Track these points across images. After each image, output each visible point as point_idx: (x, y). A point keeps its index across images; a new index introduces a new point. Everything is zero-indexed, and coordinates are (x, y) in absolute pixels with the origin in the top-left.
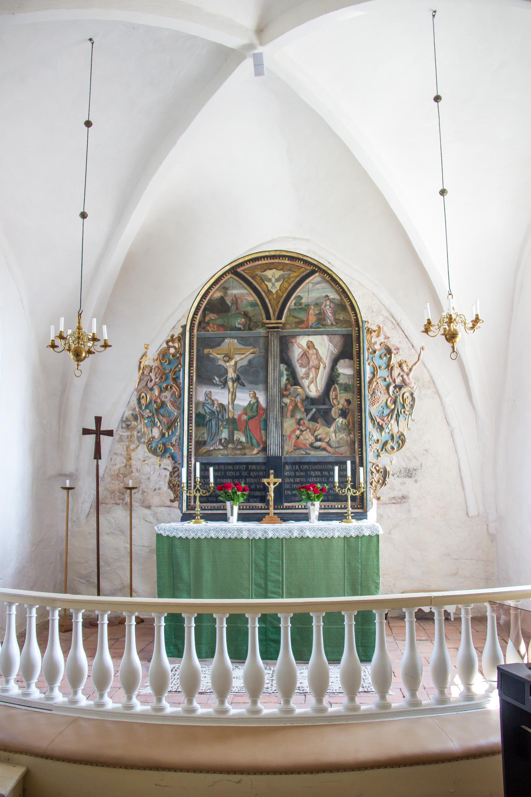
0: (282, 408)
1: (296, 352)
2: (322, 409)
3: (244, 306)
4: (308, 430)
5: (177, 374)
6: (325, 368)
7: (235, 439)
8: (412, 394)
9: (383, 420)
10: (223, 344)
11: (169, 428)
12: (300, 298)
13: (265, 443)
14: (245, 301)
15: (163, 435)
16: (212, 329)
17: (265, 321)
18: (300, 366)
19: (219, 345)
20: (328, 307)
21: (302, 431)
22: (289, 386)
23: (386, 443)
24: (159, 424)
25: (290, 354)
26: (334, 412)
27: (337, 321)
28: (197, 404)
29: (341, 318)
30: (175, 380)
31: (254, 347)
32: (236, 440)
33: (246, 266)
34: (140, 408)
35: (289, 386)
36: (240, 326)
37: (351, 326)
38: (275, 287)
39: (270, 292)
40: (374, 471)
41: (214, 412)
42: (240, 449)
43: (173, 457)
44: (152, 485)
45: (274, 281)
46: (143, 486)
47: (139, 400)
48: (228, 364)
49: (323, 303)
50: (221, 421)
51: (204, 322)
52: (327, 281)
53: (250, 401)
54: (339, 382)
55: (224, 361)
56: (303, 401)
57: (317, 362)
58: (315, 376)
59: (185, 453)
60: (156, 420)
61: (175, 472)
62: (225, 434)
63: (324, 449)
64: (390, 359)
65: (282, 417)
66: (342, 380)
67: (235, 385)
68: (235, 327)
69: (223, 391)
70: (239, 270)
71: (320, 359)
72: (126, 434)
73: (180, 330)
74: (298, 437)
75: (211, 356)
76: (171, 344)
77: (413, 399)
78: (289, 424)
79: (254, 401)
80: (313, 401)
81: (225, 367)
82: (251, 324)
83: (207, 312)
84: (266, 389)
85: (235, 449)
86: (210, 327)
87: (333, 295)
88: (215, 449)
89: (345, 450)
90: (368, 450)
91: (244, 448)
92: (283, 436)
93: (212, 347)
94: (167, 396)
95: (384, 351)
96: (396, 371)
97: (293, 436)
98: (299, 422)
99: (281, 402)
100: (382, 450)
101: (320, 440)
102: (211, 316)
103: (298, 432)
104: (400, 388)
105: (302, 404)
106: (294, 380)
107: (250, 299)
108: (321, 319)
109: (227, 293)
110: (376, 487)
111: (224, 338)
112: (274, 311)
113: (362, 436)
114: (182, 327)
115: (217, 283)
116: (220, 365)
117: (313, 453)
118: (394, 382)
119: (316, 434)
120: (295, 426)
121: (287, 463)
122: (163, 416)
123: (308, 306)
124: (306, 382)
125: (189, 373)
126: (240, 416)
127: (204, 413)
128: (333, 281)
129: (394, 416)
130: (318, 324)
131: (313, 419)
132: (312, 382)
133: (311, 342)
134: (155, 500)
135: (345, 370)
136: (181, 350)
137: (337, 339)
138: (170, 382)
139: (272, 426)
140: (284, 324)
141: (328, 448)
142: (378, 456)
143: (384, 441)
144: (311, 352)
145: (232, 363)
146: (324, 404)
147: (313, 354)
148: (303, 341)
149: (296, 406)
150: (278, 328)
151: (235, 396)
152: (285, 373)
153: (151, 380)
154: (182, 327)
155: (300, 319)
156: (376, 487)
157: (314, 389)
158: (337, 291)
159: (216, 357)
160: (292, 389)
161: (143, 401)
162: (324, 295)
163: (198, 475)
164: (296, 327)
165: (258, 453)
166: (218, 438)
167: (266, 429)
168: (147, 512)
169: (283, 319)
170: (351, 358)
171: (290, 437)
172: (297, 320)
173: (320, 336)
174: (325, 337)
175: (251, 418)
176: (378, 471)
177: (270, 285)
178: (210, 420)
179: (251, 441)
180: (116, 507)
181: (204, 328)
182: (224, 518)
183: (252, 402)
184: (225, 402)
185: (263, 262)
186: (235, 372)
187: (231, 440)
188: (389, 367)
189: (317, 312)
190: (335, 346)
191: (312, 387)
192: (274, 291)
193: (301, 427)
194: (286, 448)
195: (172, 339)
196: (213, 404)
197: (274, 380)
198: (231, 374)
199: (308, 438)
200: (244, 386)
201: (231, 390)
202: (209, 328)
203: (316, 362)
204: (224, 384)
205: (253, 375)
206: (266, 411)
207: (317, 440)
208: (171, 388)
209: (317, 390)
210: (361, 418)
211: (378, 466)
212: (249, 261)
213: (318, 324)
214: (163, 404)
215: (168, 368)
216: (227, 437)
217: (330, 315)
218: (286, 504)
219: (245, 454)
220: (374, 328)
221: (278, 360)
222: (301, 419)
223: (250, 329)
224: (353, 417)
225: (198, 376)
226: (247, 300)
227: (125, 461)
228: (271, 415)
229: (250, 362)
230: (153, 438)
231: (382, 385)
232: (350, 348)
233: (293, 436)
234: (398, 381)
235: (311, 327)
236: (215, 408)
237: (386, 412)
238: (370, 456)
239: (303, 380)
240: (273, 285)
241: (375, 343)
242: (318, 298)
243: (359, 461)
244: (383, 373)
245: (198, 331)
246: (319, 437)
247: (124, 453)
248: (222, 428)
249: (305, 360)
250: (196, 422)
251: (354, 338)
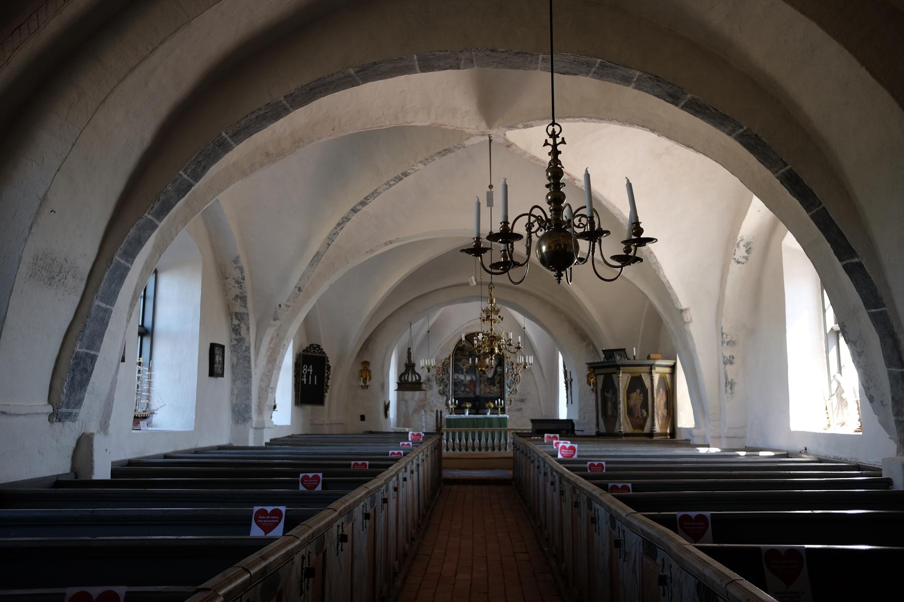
78: (482, 386)
94: (445, 377)
135: (499, 369)
157: (490, 375)
199: (488, 390)
238: (507, 396)
243: (503, 398)
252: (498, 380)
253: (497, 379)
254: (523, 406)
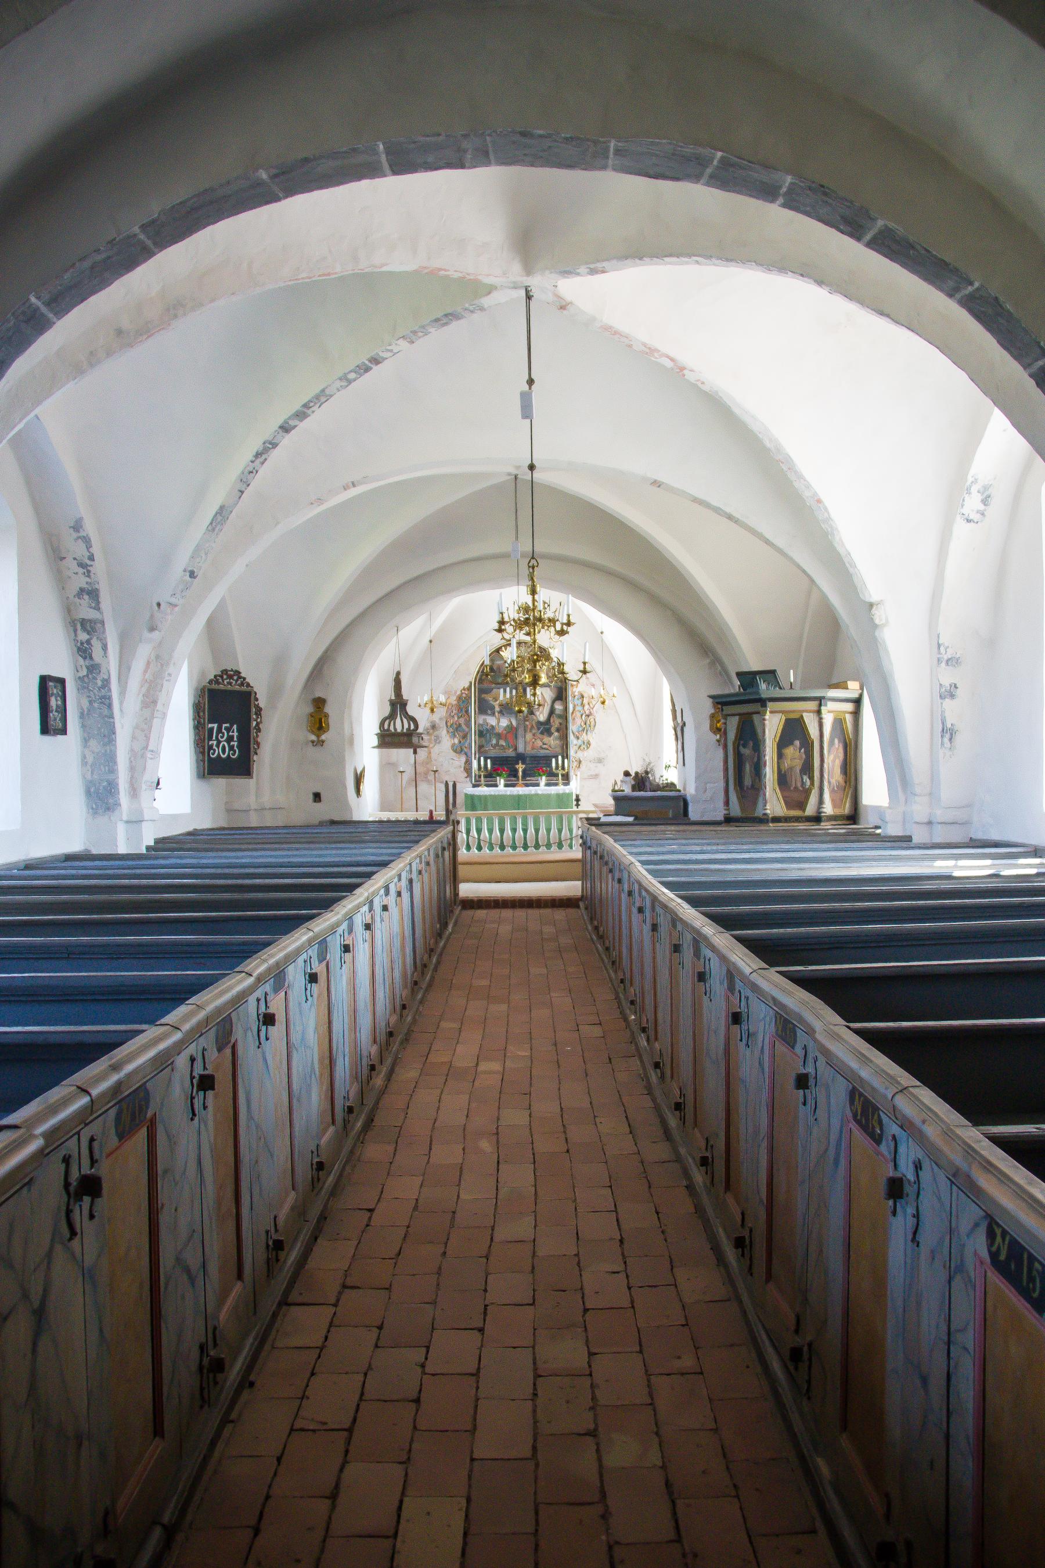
26: (553, 730)
30: (467, 712)
61: (468, 762)
62: (494, 742)
66: (557, 712)
78: (529, 736)
80: (540, 723)
89: (558, 750)
96: (586, 707)
117: (542, 751)
124: (537, 713)
131: (542, 733)
135: (559, 707)
137: (555, 690)
139: (519, 736)
149: (532, 727)
157: (542, 716)
182: (496, 786)
184: (494, 724)
187: (497, 744)
188: (583, 705)
195: (464, 689)
198: (497, 709)
199: (539, 743)
204: (493, 714)
206: (516, 729)
214: (460, 725)
231: (579, 714)
232: (561, 695)
238: (572, 752)
243: (566, 756)
244: (579, 708)
252: (557, 725)
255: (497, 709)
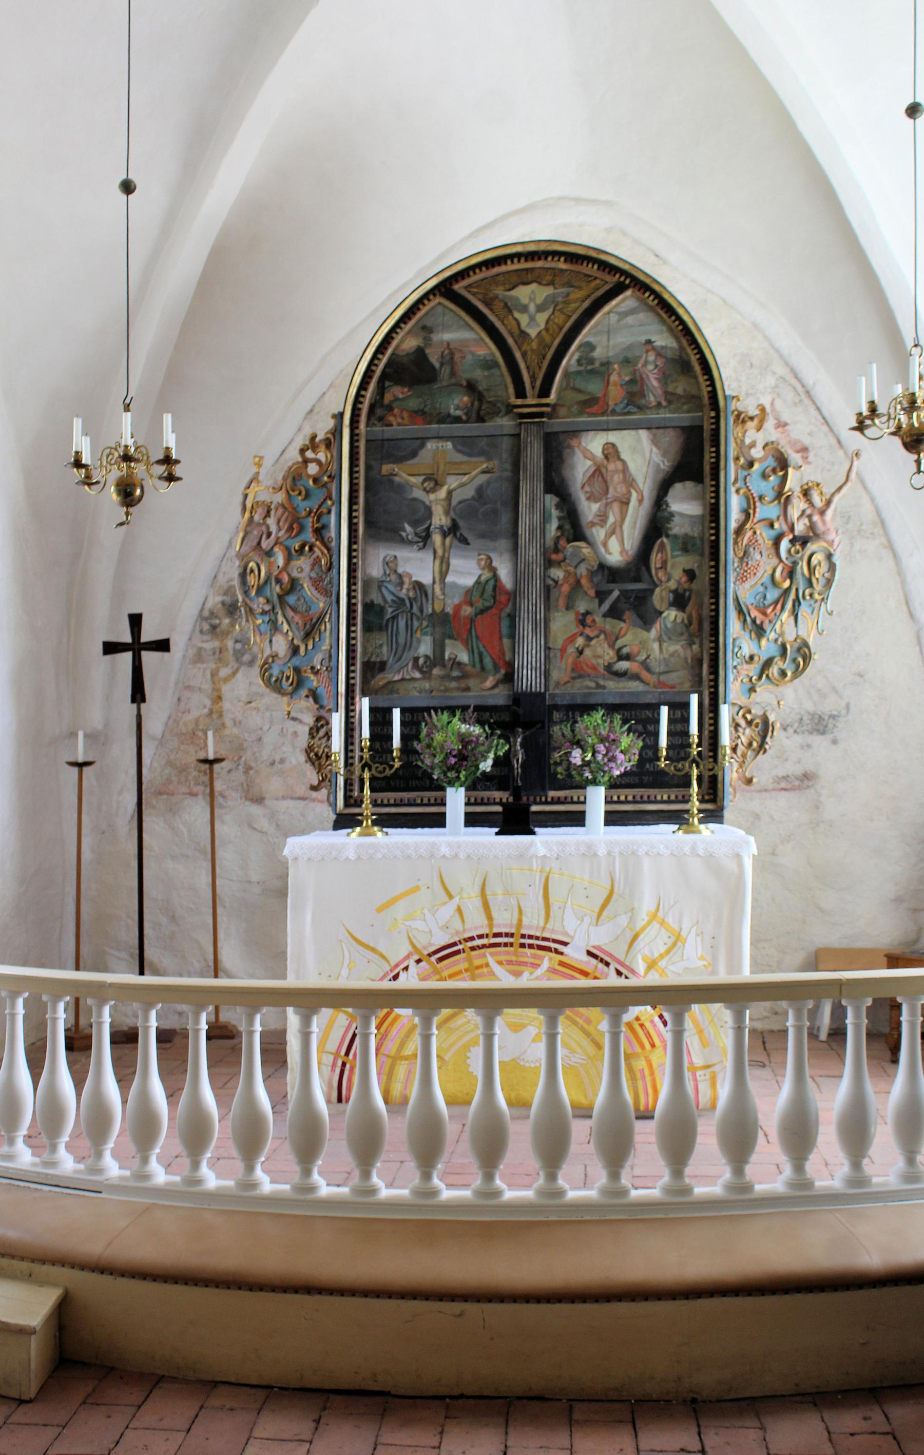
0: (547, 590)
1: (579, 469)
2: (633, 591)
3: (468, 369)
4: (602, 637)
5: (324, 520)
6: (641, 501)
7: (447, 657)
8: (829, 556)
9: (765, 614)
10: (422, 453)
11: (307, 635)
12: (590, 347)
13: (510, 665)
14: (469, 357)
15: (295, 651)
16: (400, 420)
17: (514, 401)
18: (588, 499)
19: (414, 454)
20: (651, 367)
21: (589, 639)
22: (562, 542)
23: (768, 663)
24: (286, 627)
25: (566, 473)
26: (660, 598)
27: (671, 398)
28: (367, 584)
29: (680, 391)
30: (319, 532)
31: (489, 459)
32: (450, 659)
33: (473, 278)
34: (246, 593)
35: (562, 542)
36: (458, 413)
37: (700, 408)
38: (534, 323)
39: (524, 334)
40: (743, 723)
41: (402, 600)
42: (457, 679)
43: (314, 695)
44: (265, 754)
45: (533, 310)
46: (247, 756)
47: (243, 576)
48: (432, 497)
49: (640, 357)
50: (418, 619)
51: (382, 405)
52: (651, 309)
53: (480, 576)
54: (670, 533)
55: (425, 489)
56: (592, 574)
57: (624, 490)
58: (619, 520)
59: (342, 688)
60: (280, 618)
61: (320, 726)
63: (636, 677)
64: (784, 478)
65: (548, 608)
66: (677, 528)
67: (448, 540)
68: (449, 415)
69: (421, 555)
70: (456, 287)
71: (630, 482)
72: (211, 645)
73: (331, 423)
74: (581, 652)
75: (397, 479)
76: (309, 454)
77: (832, 568)
78: (563, 624)
79: (487, 575)
81: (427, 503)
82: (482, 407)
83: (387, 384)
84: (515, 549)
85: (447, 677)
86: (395, 416)
87: (664, 340)
88: (403, 680)
89: (680, 678)
90: (731, 677)
91: (465, 676)
92: (548, 648)
93: (399, 460)
94: (302, 567)
95: (771, 462)
96: (798, 506)
97: (571, 650)
98: (582, 620)
99: (545, 576)
100: (760, 678)
101: (628, 658)
102: (396, 392)
103: (580, 641)
104: (804, 541)
105: (591, 580)
106: (574, 528)
107: (481, 352)
108: (635, 394)
109: (430, 339)
110: (744, 756)
111: (423, 440)
112: (533, 378)
113: (717, 648)
114: (334, 416)
115: (410, 319)
116: (415, 499)
117: (612, 685)
118: (792, 529)
119: (619, 644)
120: (574, 629)
121: (556, 707)
122: (294, 610)
123: (607, 364)
124: (599, 534)
125: (351, 518)
126: (457, 608)
127: (382, 604)
128: (664, 307)
129: (789, 605)
130: (628, 405)
131: (614, 613)
132: (613, 532)
133: (613, 445)
134: (273, 785)
135: (684, 505)
136: (334, 468)
137: (671, 439)
138: (309, 536)
139: (526, 628)
140: (554, 407)
141: (645, 675)
142: (752, 690)
143: (764, 658)
144: (611, 467)
145: (442, 493)
146: (637, 579)
147: (616, 471)
148: (595, 443)
150: (541, 415)
151: (448, 565)
152: (555, 513)
153: (269, 535)
154: (334, 416)
155: (590, 393)
156: (744, 756)
157: (617, 550)
158: (671, 330)
159: (407, 482)
160: (570, 548)
161: (252, 580)
162: (643, 339)
163: (366, 732)
164: (581, 413)
165: (495, 686)
166: (412, 654)
167: (512, 636)
168: (255, 810)
169: (553, 395)
170: (698, 478)
171: (563, 650)
172: (582, 397)
173: (633, 432)
174: (643, 434)
175: (482, 612)
176: (749, 723)
177: (524, 319)
178: (395, 618)
179: (481, 661)
180: (189, 801)
181: (381, 419)
183: (483, 578)
184: (426, 577)
185: (510, 267)
186: (447, 513)
187: (437, 659)
188: (782, 498)
189: (627, 379)
190: (664, 454)
191: (613, 543)
192: (533, 332)
193: (588, 631)
194: (555, 675)
195: (313, 443)
196: (401, 584)
197: (532, 530)
198: (440, 519)
200: (468, 544)
201: (440, 552)
202: (391, 419)
203: (621, 489)
204: (425, 539)
205: (484, 519)
206: (513, 596)
207: (621, 658)
208: (311, 549)
209: (623, 551)
210: (717, 610)
211: (749, 712)
212: (480, 265)
213: (628, 405)
214: (294, 585)
215: (303, 506)
216: (429, 653)
217: (655, 383)
218: (552, 794)
219: (468, 689)
220: (753, 411)
221: (540, 486)
222: (588, 613)
223: (481, 419)
224: (700, 606)
225: (368, 523)
226: (473, 354)
227: (208, 703)
228: (524, 606)
229: (480, 491)
230: (274, 656)
231: (765, 536)
232: (697, 457)
233: (571, 650)
234: (800, 527)
235: (614, 412)
236: (404, 591)
237: (772, 595)
239: (594, 530)
240: (532, 319)
241: (753, 445)
242: (630, 347)
244: (768, 510)
245: (367, 425)
246: (625, 651)
247: (207, 686)
248: (418, 634)
249: (598, 485)
250: (364, 621)
251: (707, 435)
253: (672, 568)
254: (822, 755)
255: (440, 519)
